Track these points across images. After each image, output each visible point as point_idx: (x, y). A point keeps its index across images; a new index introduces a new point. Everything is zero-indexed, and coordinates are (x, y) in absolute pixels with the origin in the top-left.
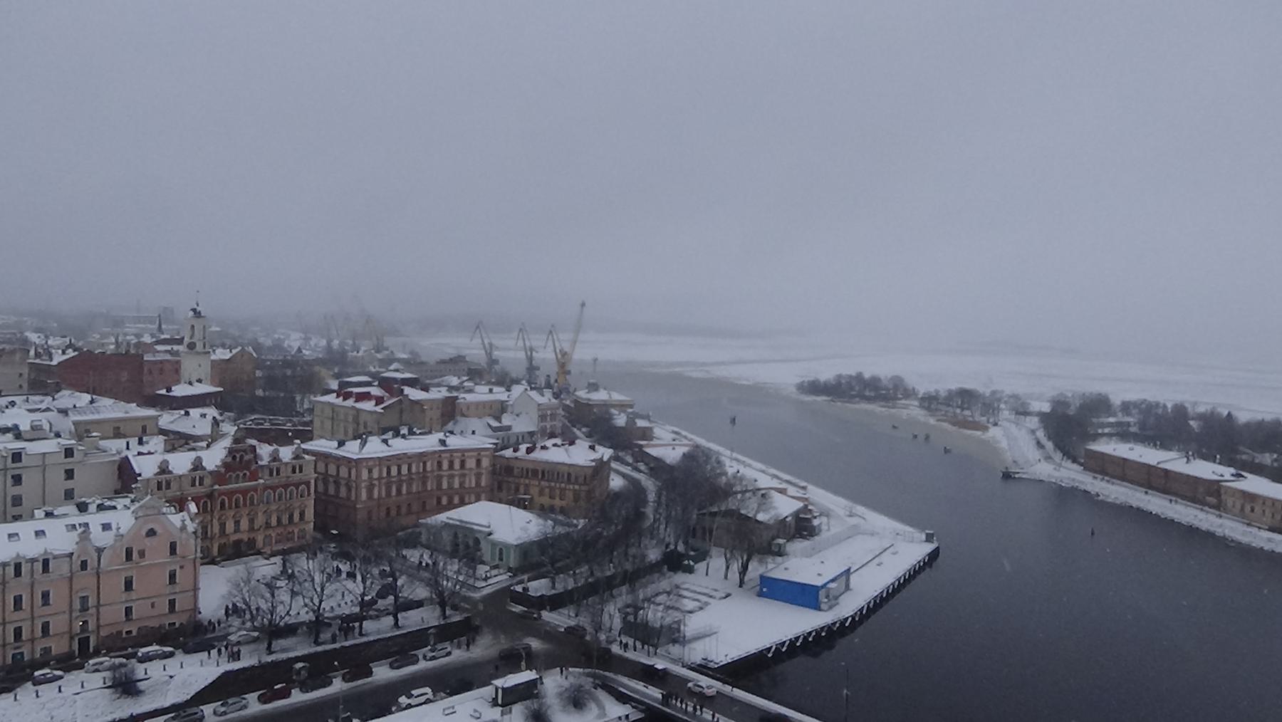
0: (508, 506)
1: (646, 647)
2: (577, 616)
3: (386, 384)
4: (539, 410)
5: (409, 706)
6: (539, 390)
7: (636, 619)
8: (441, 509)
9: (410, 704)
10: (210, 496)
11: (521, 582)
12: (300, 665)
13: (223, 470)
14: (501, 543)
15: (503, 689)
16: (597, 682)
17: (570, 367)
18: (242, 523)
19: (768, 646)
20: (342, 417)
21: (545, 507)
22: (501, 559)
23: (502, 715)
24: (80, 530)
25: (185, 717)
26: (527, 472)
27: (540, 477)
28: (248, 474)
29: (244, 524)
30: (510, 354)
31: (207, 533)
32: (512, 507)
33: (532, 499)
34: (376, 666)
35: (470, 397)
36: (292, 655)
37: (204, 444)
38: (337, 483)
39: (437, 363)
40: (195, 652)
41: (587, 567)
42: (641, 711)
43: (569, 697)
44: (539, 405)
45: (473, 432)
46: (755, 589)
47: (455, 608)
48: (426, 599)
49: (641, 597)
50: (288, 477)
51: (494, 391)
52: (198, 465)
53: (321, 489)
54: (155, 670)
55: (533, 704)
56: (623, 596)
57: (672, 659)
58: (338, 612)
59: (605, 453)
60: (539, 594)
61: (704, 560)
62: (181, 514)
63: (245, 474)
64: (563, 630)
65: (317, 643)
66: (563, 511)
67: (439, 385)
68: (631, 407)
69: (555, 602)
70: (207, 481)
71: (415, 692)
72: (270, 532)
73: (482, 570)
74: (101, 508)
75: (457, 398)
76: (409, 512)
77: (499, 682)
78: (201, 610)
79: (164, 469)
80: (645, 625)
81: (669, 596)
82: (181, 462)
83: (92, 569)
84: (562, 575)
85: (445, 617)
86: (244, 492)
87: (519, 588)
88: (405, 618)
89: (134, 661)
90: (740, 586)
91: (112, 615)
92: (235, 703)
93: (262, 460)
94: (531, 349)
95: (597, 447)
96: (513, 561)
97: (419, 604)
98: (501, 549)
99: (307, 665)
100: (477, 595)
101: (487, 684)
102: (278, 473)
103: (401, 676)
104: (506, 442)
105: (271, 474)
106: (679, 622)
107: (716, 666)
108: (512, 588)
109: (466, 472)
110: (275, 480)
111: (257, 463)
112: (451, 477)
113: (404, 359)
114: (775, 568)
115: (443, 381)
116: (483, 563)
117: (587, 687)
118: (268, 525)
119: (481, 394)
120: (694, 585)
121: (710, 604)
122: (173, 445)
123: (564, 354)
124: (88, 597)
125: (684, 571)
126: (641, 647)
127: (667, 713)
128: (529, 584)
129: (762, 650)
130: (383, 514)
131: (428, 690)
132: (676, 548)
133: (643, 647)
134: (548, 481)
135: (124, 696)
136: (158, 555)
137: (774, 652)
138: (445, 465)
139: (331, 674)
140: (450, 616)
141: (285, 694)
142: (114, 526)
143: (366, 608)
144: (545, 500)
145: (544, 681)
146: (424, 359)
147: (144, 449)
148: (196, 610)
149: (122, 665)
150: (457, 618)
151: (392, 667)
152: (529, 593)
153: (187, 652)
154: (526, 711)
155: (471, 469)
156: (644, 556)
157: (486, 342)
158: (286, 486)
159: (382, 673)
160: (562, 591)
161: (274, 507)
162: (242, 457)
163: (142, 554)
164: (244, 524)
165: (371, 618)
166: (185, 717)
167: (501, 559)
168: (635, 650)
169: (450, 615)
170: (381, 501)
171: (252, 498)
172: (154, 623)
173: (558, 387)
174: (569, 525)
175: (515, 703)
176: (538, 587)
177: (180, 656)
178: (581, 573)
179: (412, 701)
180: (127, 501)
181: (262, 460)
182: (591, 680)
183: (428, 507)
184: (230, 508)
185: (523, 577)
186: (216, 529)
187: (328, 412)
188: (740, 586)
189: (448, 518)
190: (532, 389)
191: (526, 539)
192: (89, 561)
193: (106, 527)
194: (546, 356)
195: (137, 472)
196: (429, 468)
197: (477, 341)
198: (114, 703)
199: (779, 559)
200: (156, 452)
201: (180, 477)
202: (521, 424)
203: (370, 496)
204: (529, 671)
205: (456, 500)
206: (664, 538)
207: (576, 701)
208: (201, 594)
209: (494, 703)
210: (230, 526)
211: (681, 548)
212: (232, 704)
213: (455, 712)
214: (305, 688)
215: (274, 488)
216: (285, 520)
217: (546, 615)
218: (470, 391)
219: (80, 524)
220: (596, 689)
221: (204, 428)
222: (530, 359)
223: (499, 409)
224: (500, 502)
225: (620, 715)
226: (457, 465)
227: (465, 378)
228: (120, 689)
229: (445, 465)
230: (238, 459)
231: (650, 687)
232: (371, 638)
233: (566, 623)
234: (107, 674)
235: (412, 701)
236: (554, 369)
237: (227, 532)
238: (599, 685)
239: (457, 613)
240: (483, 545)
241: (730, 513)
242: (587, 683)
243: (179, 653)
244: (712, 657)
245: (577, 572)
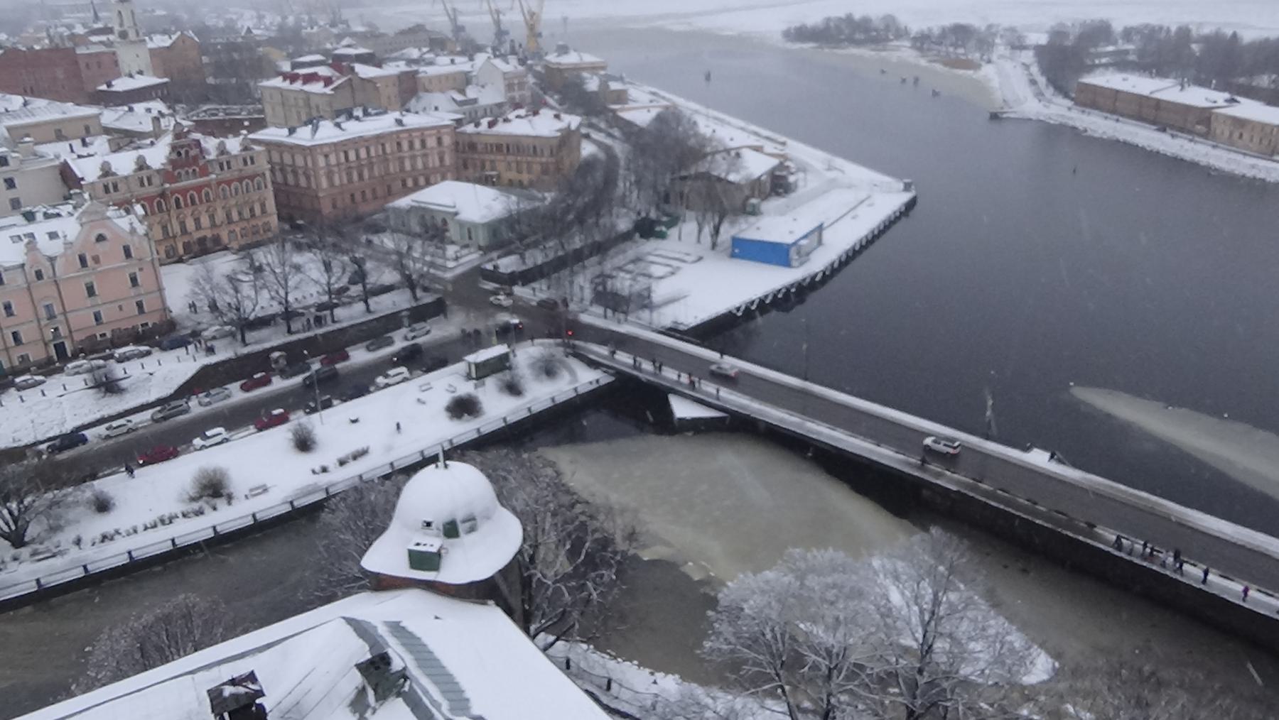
3: (339, 63)
4: (505, 79)
5: (387, 385)
6: (503, 57)
8: (406, 191)
10: (163, 195)
11: (491, 260)
12: (276, 354)
13: (170, 168)
14: (467, 223)
17: (539, 29)
18: (202, 220)
20: (292, 101)
22: (470, 238)
24: (26, 240)
25: (169, 410)
26: (492, 149)
27: (505, 151)
28: (197, 170)
29: (205, 221)
30: (477, 22)
31: (168, 234)
33: (499, 177)
34: (352, 350)
35: (431, 71)
36: (267, 345)
37: (148, 141)
38: (295, 172)
39: (396, 34)
40: (172, 349)
42: (612, 375)
44: (505, 74)
45: (436, 109)
47: (426, 289)
50: (241, 170)
51: (456, 61)
52: (142, 165)
53: (279, 178)
54: (133, 367)
55: (506, 376)
56: (592, 267)
58: (311, 301)
59: (573, 121)
60: (509, 271)
62: (132, 216)
63: (194, 170)
64: (534, 304)
65: (290, 332)
66: (532, 184)
67: (396, 59)
68: (603, 68)
69: (526, 277)
70: (156, 180)
72: (232, 227)
73: (451, 250)
74: (47, 216)
75: (416, 72)
76: (375, 198)
78: (172, 308)
79: (106, 171)
82: (124, 163)
83: (49, 278)
86: (198, 189)
87: (489, 267)
88: (376, 303)
89: (112, 361)
91: (81, 321)
92: (218, 394)
93: (209, 154)
94: (498, 12)
95: (563, 116)
96: (482, 238)
99: (284, 353)
100: (449, 275)
102: (229, 168)
104: (473, 115)
105: (222, 169)
109: (428, 151)
110: (227, 175)
111: (204, 157)
112: (413, 158)
113: (361, 33)
115: (403, 54)
116: (453, 243)
118: (230, 220)
119: (443, 65)
122: (119, 144)
123: (532, 14)
124: (51, 305)
130: (348, 200)
134: (513, 154)
135: (108, 394)
136: (113, 260)
138: (405, 146)
139: (307, 361)
141: (266, 382)
142: (60, 234)
143: (337, 297)
144: (512, 175)
146: (382, 31)
147: (84, 151)
148: (165, 309)
149: (99, 367)
150: (427, 299)
151: (368, 349)
153: (164, 349)
155: (432, 148)
157: (449, 6)
158: (240, 180)
159: (359, 356)
161: (233, 202)
162: (187, 152)
163: (96, 260)
164: (205, 221)
165: (344, 304)
166: (169, 410)
167: (470, 238)
171: (207, 194)
172: (125, 325)
173: (523, 52)
176: (508, 264)
177: (157, 354)
180: (69, 208)
181: (209, 154)
184: (186, 205)
186: (177, 229)
187: (277, 98)
189: (413, 201)
190: (496, 56)
192: (43, 271)
193: (53, 235)
194: (514, 19)
195: (80, 176)
196: (388, 150)
197: (439, 7)
198: (100, 402)
200: (96, 153)
201: (126, 178)
202: (489, 96)
203: (331, 184)
205: (422, 181)
207: (548, 370)
208: (167, 293)
209: (469, 377)
210: (190, 225)
212: (214, 395)
214: (285, 374)
215: (229, 183)
216: (247, 214)
217: (518, 290)
218: (431, 63)
219: (25, 235)
220: (567, 356)
221: (148, 127)
222: (497, 23)
223: (465, 80)
224: (468, 180)
225: (591, 379)
226: (417, 144)
227: (425, 50)
228: (103, 389)
229: (405, 146)
230: (183, 155)
232: (345, 325)
234: (85, 376)
236: (519, 34)
237: (189, 230)
242: (559, 352)
243: (156, 351)
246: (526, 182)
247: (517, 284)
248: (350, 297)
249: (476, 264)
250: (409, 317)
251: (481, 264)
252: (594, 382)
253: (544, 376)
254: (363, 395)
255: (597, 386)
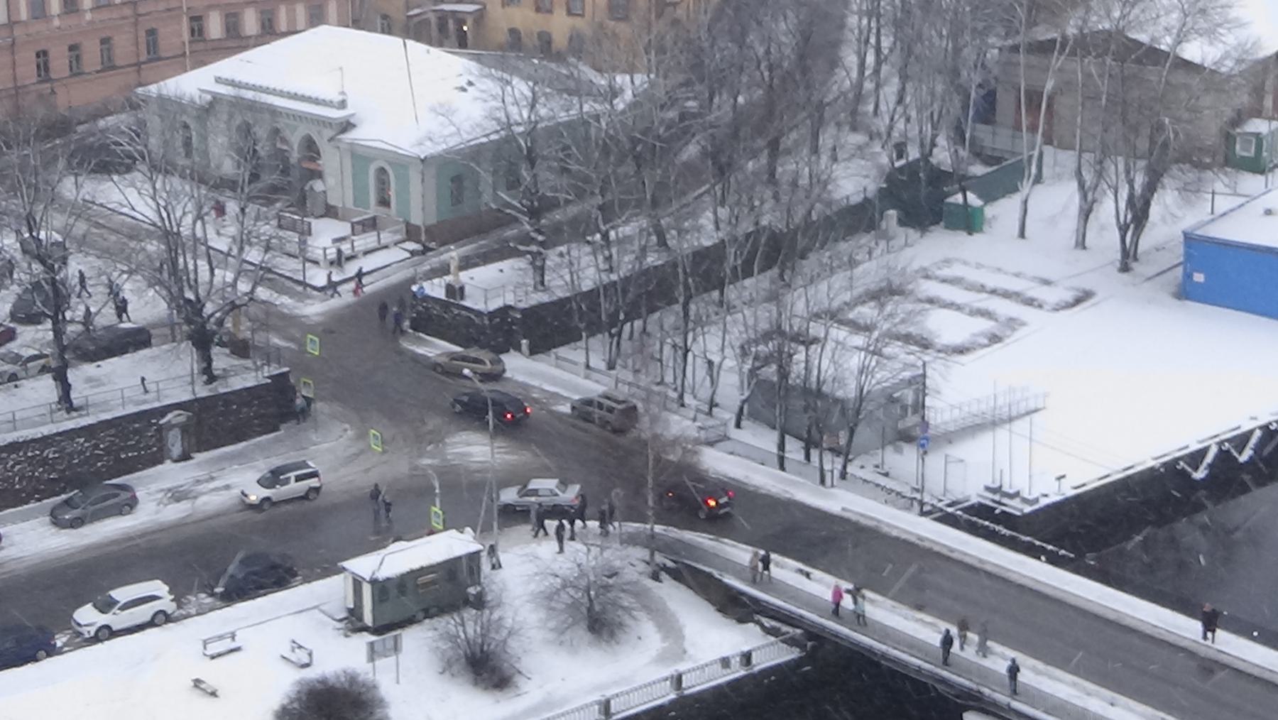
0: (399, 41)
1: (815, 454)
2: (611, 366)
7: (784, 374)
9: (107, 627)
11: (443, 270)
15: (373, 582)
16: (659, 558)
19: (1195, 447)
21: (525, 40)
22: (384, 202)
23: (371, 659)
32: (410, 43)
33: (480, 17)
41: (644, 222)
42: (792, 642)
43: (574, 606)
46: (1169, 275)
47: (241, 349)
48: (155, 325)
49: (800, 307)
55: (468, 624)
57: (890, 491)
60: (495, 304)
61: (1016, 190)
64: (565, 409)
66: (577, 46)
71: (122, 594)
76: (109, 65)
77: (364, 565)
80: (814, 395)
81: (882, 306)
84: (563, 249)
85: (212, 379)
87: (435, 289)
88: (89, 380)
90: (1125, 268)
97: (138, 340)
98: (382, 171)
101: (330, 568)
103: (88, 548)
106: (919, 383)
107: (1028, 509)
108: (415, 288)
114: (1242, 205)
116: (330, 212)
117: (630, 574)
120: (979, 266)
121: (1023, 324)
125: (952, 226)
126: (801, 456)
127: (858, 644)
128: (464, 276)
129: (1177, 460)
131: (158, 587)
132: (926, 156)
133: (808, 457)
137: (1210, 466)
140: (226, 374)
145: (503, 557)
150: (249, 380)
151: (57, 522)
152: (466, 303)
154: (444, 646)
156: (821, 182)
160: (561, 294)
167: (384, 202)
168: (782, 468)
169: (226, 374)
170: (18, 32)
174: (578, 90)
175: (409, 621)
178: (627, 239)
179: (117, 619)
182: (643, 553)
183: (165, 47)
185: (445, 257)
188: (1125, 268)
189: (218, 80)
191: (452, 142)
199: (1251, 183)
204: (453, 532)
206: (891, 128)
209: (353, 622)
211: (942, 156)
213: (237, 649)
220: (655, 577)
231: (816, 573)
233: (575, 389)
235: (117, 619)
238: (665, 569)
239: (248, 363)
240: (330, 161)
241: (1085, 45)
244: (1017, 481)
245: (612, 234)
246: (560, 40)
247: (518, 348)
248: (16, 359)
249: (396, 277)
250: (184, 429)
251: (413, 281)
252: (735, 662)
253: (581, 633)
254: (35, 659)
255: (742, 673)
